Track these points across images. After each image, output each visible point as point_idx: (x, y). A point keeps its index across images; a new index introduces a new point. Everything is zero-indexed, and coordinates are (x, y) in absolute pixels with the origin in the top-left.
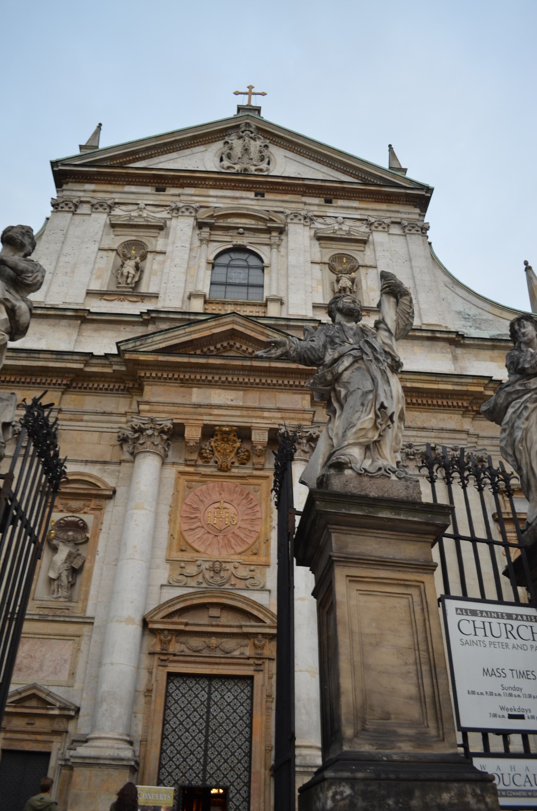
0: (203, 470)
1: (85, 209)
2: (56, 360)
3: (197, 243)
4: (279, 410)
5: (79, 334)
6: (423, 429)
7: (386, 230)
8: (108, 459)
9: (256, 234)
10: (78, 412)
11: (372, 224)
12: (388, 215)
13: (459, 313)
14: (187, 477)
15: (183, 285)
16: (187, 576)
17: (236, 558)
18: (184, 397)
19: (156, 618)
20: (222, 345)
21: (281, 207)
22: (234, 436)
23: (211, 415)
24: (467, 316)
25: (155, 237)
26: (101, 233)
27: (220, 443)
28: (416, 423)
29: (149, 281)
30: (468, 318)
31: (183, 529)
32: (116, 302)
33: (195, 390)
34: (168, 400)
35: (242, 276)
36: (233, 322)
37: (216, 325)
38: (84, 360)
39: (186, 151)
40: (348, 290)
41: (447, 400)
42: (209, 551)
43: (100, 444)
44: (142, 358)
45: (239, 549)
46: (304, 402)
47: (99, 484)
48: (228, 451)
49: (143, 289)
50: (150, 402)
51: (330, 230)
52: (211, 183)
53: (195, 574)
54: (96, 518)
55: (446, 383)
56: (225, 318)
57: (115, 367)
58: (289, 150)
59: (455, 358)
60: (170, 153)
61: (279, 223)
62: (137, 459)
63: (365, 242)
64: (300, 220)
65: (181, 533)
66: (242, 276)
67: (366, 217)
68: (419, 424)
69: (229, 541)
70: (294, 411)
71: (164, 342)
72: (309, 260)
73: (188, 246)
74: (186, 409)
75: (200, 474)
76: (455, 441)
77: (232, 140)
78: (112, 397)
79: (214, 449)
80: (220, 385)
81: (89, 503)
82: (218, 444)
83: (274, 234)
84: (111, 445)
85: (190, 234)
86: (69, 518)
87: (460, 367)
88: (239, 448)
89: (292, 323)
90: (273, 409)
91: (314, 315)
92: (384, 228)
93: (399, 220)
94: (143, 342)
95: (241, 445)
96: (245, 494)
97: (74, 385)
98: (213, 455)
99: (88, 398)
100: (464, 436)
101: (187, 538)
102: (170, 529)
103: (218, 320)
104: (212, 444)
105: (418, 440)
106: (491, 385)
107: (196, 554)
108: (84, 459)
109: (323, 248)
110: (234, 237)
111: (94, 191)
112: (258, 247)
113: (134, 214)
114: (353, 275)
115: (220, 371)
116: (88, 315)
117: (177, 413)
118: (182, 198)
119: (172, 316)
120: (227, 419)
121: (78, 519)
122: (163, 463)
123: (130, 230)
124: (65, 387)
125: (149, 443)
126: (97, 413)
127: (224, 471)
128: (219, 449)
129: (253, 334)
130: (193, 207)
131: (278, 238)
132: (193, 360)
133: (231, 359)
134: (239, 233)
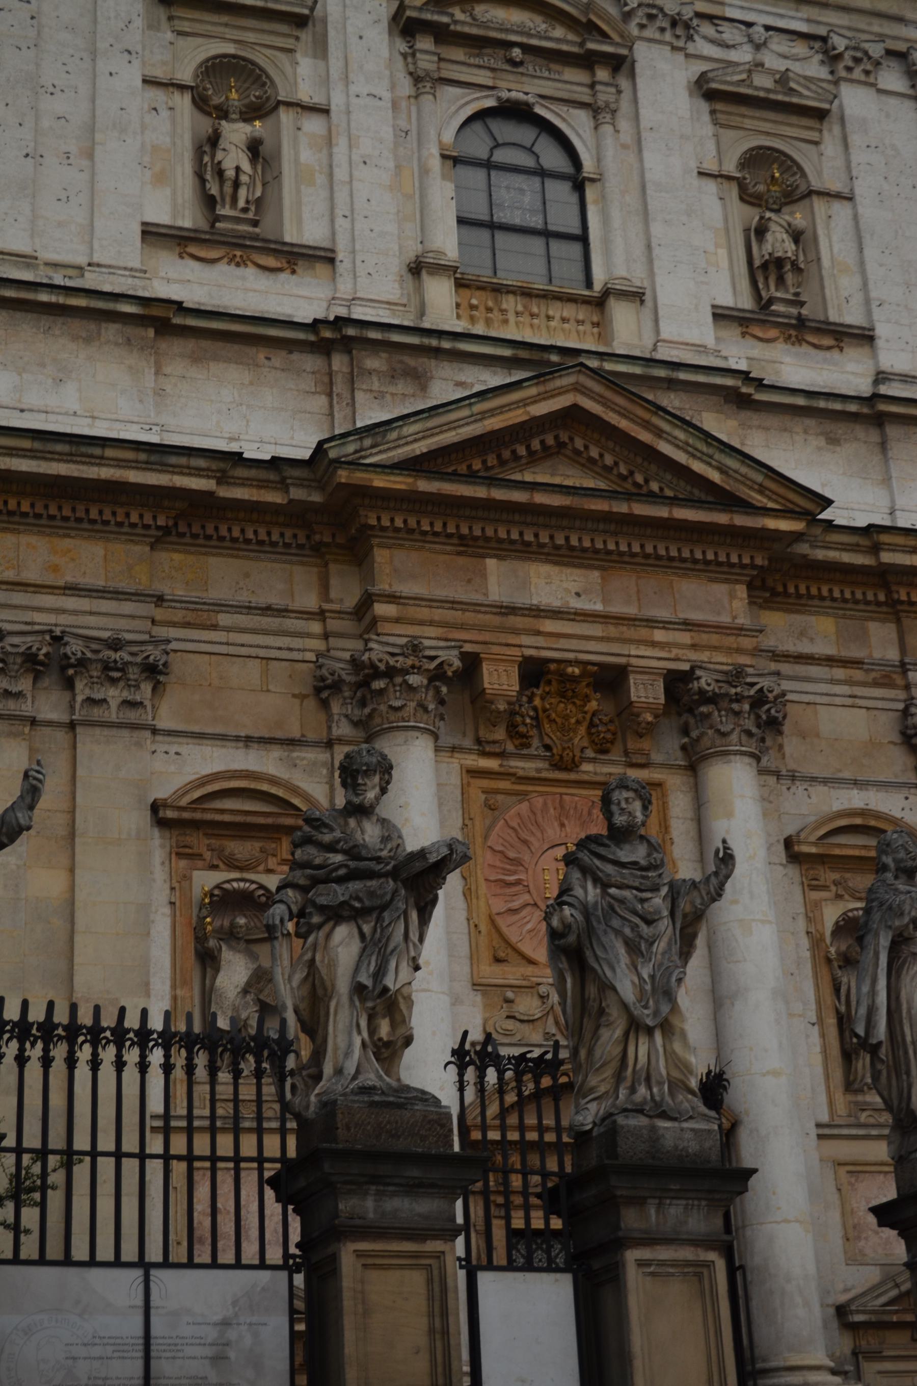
0: (519, 765)
2: (147, 466)
3: (406, 86)
7: (871, 80)
8: (296, 734)
9: (553, 66)
10: (204, 603)
11: (838, 57)
12: (877, 27)
14: (486, 783)
16: (522, 1021)
18: (469, 581)
20: (542, 442)
22: (588, 685)
23: (538, 633)
25: (291, 51)
26: (138, 23)
27: (553, 700)
29: (299, 203)
31: (494, 911)
32: (223, 268)
34: (441, 593)
35: (527, 199)
36: (577, 388)
37: (539, 394)
38: (218, 471)
43: (268, 691)
44: (380, 482)
46: (736, 604)
47: (296, 801)
48: (573, 720)
50: (400, 597)
51: (741, 72)
53: (539, 1015)
56: (560, 376)
57: (297, 493)
61: (617, 44)
63: (821, 115)
64: (662, 30)
65: (493, 922)
66: (527, 199)
67: (822, 31)
70: (719, 628)
71: (424, 438)
72: (693, 165)
73: (387, 95)
74: (481, 616)
75: (514, 775)
78: (274, 561)
79: (540, 713)
80: (548, 554)
81: (274, 845)
82: (551, 704)
84: (294, 696)
85: (385, 53)
86: (235, 885)
89: (683, 376)
90: (675, 623)
91: (718, 339)
93: (902, 47)
94: (379, 439)
97: (182, 528)
99: (212, 560)
101: (505, 930)
102: (469, 909)
103: (544, 382)
107: (530, 970)
108: (243, 734)
109: (722, 126)
110: (499, 74)
112: (562, 109)
114: (798, 219)
117: (462, 627)
119: (396, 338)
120: (574, 644)
121: (254, 886)
122: (437, 750)
123: (215, 18)
125: (413, 704)
126: (249, 609)
127: (567, 769)
128: (553, 716)
129: (623, 424)
132: (499, 494)
133: (585, 495)
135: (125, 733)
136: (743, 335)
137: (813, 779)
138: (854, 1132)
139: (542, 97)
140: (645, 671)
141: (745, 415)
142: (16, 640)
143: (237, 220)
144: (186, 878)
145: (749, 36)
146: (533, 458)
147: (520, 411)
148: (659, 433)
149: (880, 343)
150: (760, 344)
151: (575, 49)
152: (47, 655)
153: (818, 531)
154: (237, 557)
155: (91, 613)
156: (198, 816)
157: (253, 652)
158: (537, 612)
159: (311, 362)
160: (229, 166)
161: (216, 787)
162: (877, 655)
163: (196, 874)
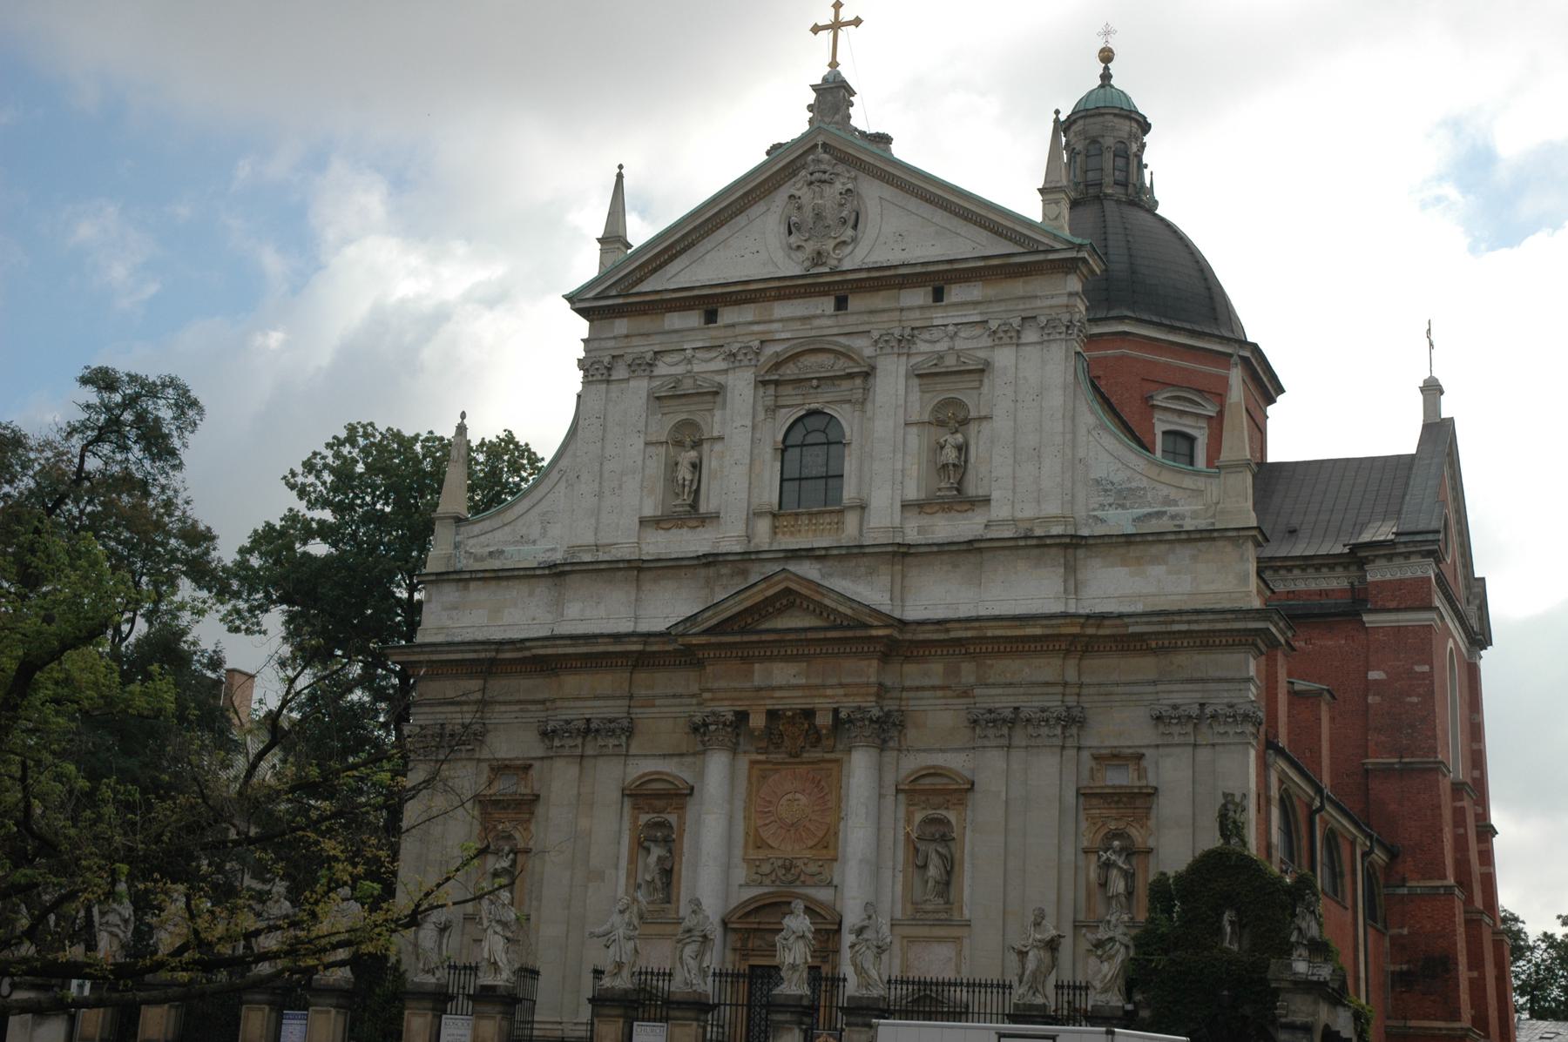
1: (620, 372)
2: (615, 643)
3: (761, 415)
4: (841, 685)
5: (638, 588)
6: (1011, 685)
7: (1014, 341)
9: (837, 382)
13: (1098, 482)
15: (745, 496)
19: (732, 920)
21: (868, 323)
24: (1109, 487)
29: (709, 490)
30: (1111, 490)
32: (674, 531)
36: (786, 579)
39: (739, 217)
40: (951, 467)
44: (695, 641)
45: (811, 843)
49: (703, 509)
52: (773, 294)
54: (679, 817)
55: (1034, 626)
58: (887, 183)
59: (1071, 569)
60: (718, 228)
62: (709, 753)
63: (982, 371)
65: (757, 830)
68: (1008, 681)
69: (801, 835)
72: (902, 422)
73: (749, 424)
77: (798, 190)
83: (858, 382)
88: (807, 731)
89: (867, 550)
92: (1011, 338)
100: (1059, 689)
101: (762, 833)
104: (781, 728)
106: (1091, 621)
111: (627, 336)
113: (680, 369)
114: (959, 438)
118: (738, 330)
126: (667, 697)
130: (751, 347)
131: (861, 391)
132: (746, 638)
134: (812, 387)
136: (920, 513)
137: (918, 750)
138: (910, 922)
139: (828, 402)
140: (822, 709)
141: (908, 560)
143: (682, 505)
144: (636, 819)
145: (946, 332)
146: (780, 612)
148: (823, 595)
151: (843, 373)
153: (914, 627)
156: (639, 792)
157: (668, 715)
158: (773, 689)
159: (703, 572)
160: (680, 477)
161: (646, 779)
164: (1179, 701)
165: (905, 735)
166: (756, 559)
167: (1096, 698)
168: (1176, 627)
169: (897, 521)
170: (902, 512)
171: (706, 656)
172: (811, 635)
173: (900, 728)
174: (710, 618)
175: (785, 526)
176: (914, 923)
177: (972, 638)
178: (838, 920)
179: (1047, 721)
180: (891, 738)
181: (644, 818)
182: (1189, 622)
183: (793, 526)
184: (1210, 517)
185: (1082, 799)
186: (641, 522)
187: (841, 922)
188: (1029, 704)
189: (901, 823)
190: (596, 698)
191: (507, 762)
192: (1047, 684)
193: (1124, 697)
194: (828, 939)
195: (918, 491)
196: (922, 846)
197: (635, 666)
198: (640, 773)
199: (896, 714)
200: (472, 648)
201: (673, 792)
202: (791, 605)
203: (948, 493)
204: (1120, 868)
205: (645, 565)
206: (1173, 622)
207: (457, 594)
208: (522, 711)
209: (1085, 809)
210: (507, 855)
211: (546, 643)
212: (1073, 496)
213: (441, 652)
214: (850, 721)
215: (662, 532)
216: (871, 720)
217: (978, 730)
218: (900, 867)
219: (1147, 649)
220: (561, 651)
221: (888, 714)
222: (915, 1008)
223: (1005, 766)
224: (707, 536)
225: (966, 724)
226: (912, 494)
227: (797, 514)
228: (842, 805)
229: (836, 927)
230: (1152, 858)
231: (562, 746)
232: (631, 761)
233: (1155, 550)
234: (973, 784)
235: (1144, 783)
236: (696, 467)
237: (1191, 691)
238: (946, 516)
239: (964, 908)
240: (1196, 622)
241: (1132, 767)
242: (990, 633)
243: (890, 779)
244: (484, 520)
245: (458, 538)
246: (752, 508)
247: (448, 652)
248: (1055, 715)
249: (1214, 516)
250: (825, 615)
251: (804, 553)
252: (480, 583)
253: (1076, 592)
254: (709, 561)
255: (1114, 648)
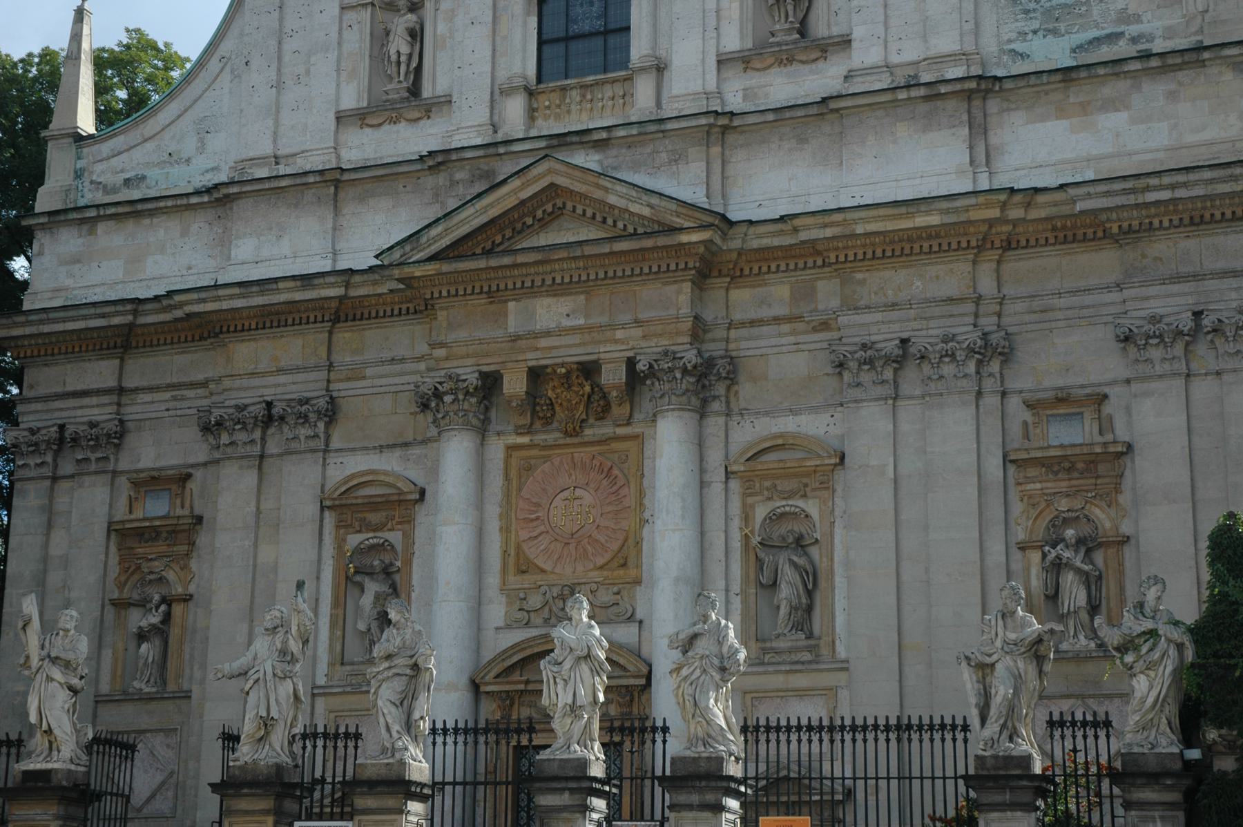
0: (539, 438)
2: (304, 288)
4: (638, 322)
6: (894, 306)
8: (410, 439)
15: (488, 68)
16: (528, 612)
17: (596, 576)
19: (487, 679)
23: (537, 349)
27: (559, 391)
28: (885, 295)
30: (1034, 10)
32: (386, 127)
33: (511, 305)
41: (940, 241)
42: (556, 570)
45: (600, 561)
48: (574, 402)
49: (426, 92)
55: (928, 213)
59: (979, 130)
65: (518, 547)
69: (584, 550)
74: (499, 345)
76: (952, 319)
84: (411, 414)
87: (986, 146)
88: (589, 397)
89: (670, 126)
95: (592, 389)
96: (606, 470)
98: (553, 409)
104: (550, 393)
105: (884, 328)
106: (1018, 198)
107: (540, 577)
115: (541, 269)
116: (341, 175)
120: (562, 352)
121: (382, 541)
124: (330, 324)
127: (571, 436)
132: (493, 262)
135: (309, 455)
136: (745, 70)
140: (611, 361)
142: (251, 409)
143: (397, 91)
144: (344, 540)
146: (543, 223)
147: (513, 199)
148: (606, 190)
149: (854, 45)
150: (758, 74)
152: (263, 416)
153: (743, 228)
154: (381, 327)
155: (294, 383)
156: (344, 502)
157: (387, 389)
158: (536, 335)
159: (430, 181)
160: (393, 52)
161: (355, 482)
162: (820, 307)
163: (349, 537)
164: (1161, 311)
165: (737, 392)
166: (504, 154)
167: (1027, 318)
168: (1152, 197)
169: (712, 85)
170: (719, 70)
171: (436, 295)
172: (588, 250)
173: (728, 382)
174: (440, 236)
175: (548, 107)
176: (761, 669)
177: (833, 238)
178: (645, 670)
179: (953, 356)
180: (715, 398)
181: (354, 540)
182: (1173, 187)
183: (559, 106)
184: (1196, 33)
185: (1012, 469)
186: (338, 119)
187: (650, 672)
188: (924, 333)
189: (736, 523)
190: (281, 371)
191: (155, 474)
192: (951, 300)
193: (1069, 313)
194: (632, 701)
195: (742, 38)
196: (767, 558)
197: (336, 320)
198: (348, 473)
199: (720, 362)
200: (99, 311)
201: (395, 498)
202: (557, 214)
203: (788, 38)
204: (1079, 571)
205: (346, 177)
206: (1148, 189)
207: (80, 241)
208: (175, 398)
209: (1019, 484)
210: (157, 608)
211: (203, 295)
212: (977, 25)
213: (55, 321)
214: (652, 372)
215: (368, 130)
216: (685, 371)
217: (846, 375)
218: (736, 587)
219: (1104, 237)
220: (225, 305)
221: (710, 363)
222: (773, 799)
223: (891, 427)
224: (433, 131)
225: (829, 370)
226: (733, 41)
227: (564, 89)
228: (646, 501)
229: (643, 681)
230: (1128, 551)
231: (232, 443)
232: (332, 459)
233: (1109, 90)
234: (842, 457)
235: (1109, 437)
236: (416, 35)
237: (1179, 295)
238: (782, 68)
239: (838, 642)
240: (1185, 185)
241: (1088, 415)
242: (860, 229)
243: (715, 458)
244: (115, 135)
245: (80, 164)
246: (498, 82)
247: (64, 320)
248: (965, 346)
249: (1201, 31)
250: (610, 221)
251: (575, 139)
252: (111, 223)
253: (988, 163)
254: (438, 161)
255: (1052, 241)
